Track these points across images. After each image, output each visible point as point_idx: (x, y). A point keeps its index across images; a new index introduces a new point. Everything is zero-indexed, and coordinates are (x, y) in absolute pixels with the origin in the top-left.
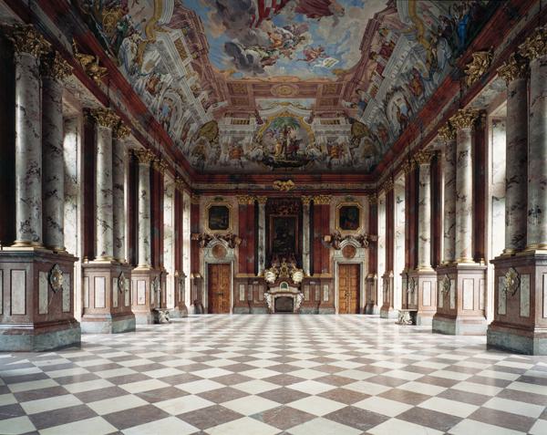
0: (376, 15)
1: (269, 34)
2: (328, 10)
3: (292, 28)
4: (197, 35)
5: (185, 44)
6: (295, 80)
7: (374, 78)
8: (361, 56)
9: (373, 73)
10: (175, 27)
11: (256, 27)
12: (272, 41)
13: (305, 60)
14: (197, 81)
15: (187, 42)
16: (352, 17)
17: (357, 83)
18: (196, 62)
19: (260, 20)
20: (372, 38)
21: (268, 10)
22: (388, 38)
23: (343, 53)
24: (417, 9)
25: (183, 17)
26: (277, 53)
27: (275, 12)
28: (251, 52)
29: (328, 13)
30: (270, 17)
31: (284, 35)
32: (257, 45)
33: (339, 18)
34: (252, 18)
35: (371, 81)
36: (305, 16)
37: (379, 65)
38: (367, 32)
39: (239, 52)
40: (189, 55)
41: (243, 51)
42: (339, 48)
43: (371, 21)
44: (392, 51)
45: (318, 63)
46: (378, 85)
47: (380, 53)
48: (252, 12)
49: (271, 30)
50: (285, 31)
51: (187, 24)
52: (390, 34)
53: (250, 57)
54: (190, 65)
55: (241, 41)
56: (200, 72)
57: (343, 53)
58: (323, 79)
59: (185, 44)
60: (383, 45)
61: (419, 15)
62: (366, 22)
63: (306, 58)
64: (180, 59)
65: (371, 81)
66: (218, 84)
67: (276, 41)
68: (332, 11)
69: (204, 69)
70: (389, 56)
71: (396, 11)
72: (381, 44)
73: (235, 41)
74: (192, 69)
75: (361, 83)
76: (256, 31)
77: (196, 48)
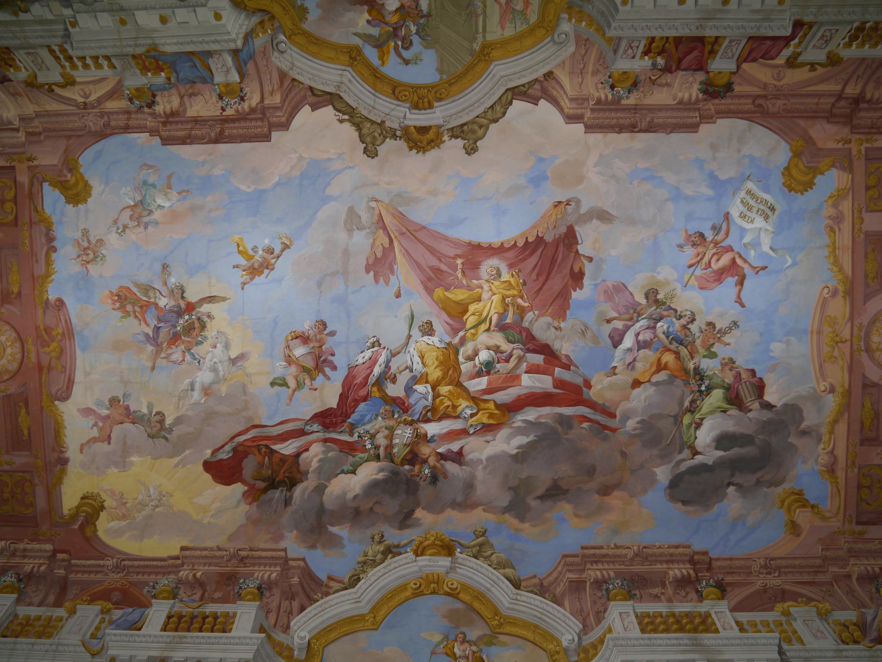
0: (571, 119)
1: (636, 384)
2: (557, 242)
3: (619, 325)
4: (637, 568)
5: (661, 607)
6: (839, 308)
7: (814, 54)
8: (719, 121)
9: (792, 63)
10: (600, 616)
11: (613, 416)
12: (662, 376)
13: (741, 283)
14: (823, 616)
15: (656, 598)
16: (580, 179)
17: (857, 101)
18: (737, 595)
19: (592, 405)
20: (651, 109)
21: (559, 383)
22: (641, 65)
23: (712, 177)
24: (521, 27)
25: (577, 586)
26: (708, 365)
27: (567, 367)
28: (705, 436)
29: (570, 238)
30: (579, 381)
31: (642, 345)
32: (677, 419)
33: (583, 211)
34: (585, 425)
35: (833, 60)
36: (577, 295)
37: (747, 57)
38: (632, 128)
39: (703, 468)
40: (703, 607)
41: (699, 458)
42: (688, 191)
43: (590, 128)
44: (678, 40)
45: (756, 244)
46: (844, 30)
47: (700, 66)
48: (565, 422)
49: (624, 377)
50: (628, 341)
51: (598, 584)
52: (623, 64)
53: (723, 441)
54: (744, 617)
55: (664, 457)
56: (783, 595)
57: (712, 177)
58: (838, 219)
59: (661, 607)
60: (667, 70)
61: (533, 18)
62: (596, 138)
63: (731, 281)
64: (707, 638)
65: (833, 60)
66: (853, 553)
67: (660, 367)
68: (563, 229)
69: (774, 581)
70: (701, 40)
71: (549, 75)
72: (668, 78)
73: (663, 474)
74: (758, 616)
75: (852, 90)
76: (626, 418)
77: (683, 583)
